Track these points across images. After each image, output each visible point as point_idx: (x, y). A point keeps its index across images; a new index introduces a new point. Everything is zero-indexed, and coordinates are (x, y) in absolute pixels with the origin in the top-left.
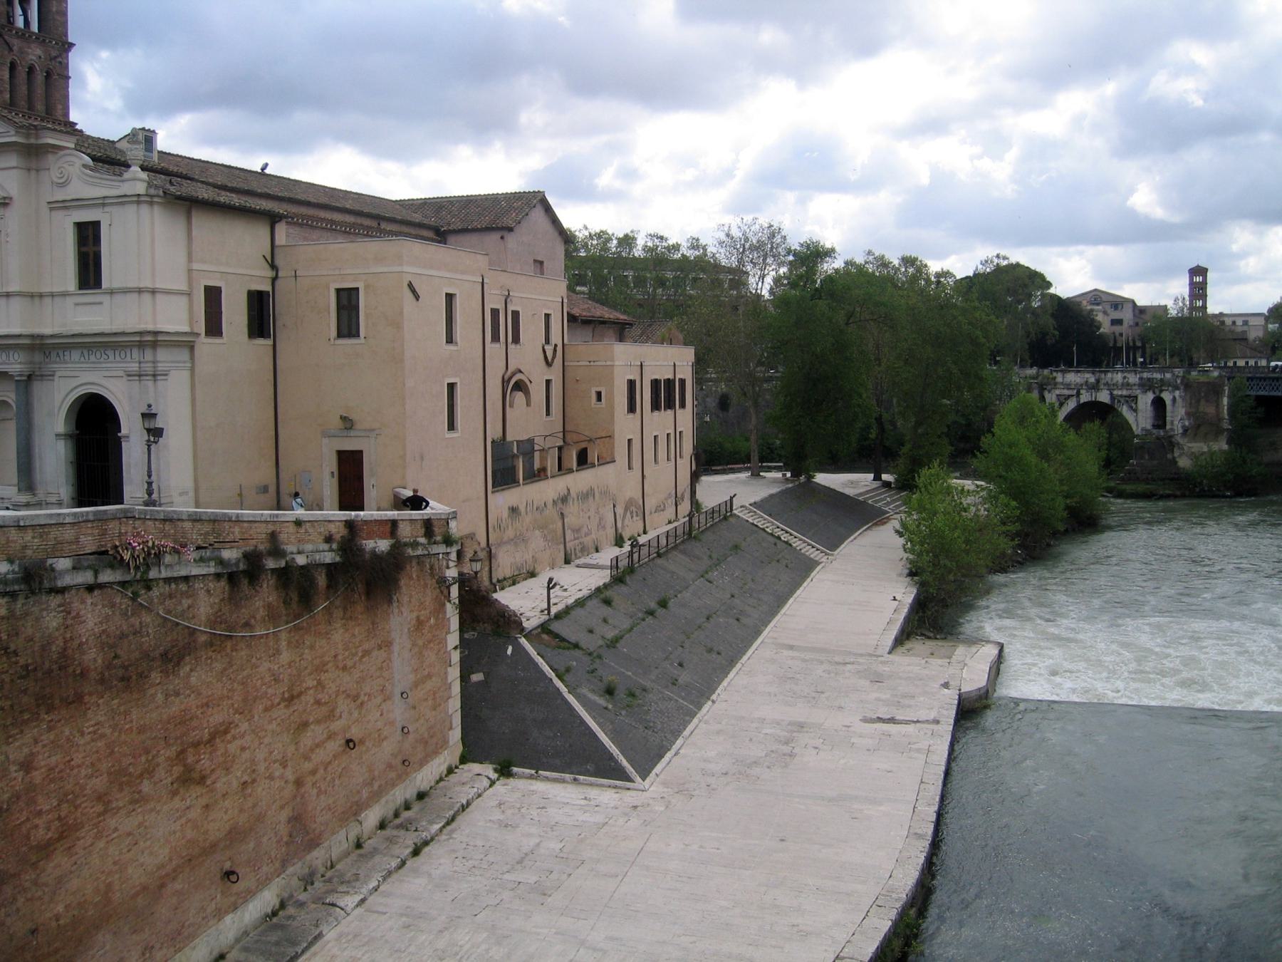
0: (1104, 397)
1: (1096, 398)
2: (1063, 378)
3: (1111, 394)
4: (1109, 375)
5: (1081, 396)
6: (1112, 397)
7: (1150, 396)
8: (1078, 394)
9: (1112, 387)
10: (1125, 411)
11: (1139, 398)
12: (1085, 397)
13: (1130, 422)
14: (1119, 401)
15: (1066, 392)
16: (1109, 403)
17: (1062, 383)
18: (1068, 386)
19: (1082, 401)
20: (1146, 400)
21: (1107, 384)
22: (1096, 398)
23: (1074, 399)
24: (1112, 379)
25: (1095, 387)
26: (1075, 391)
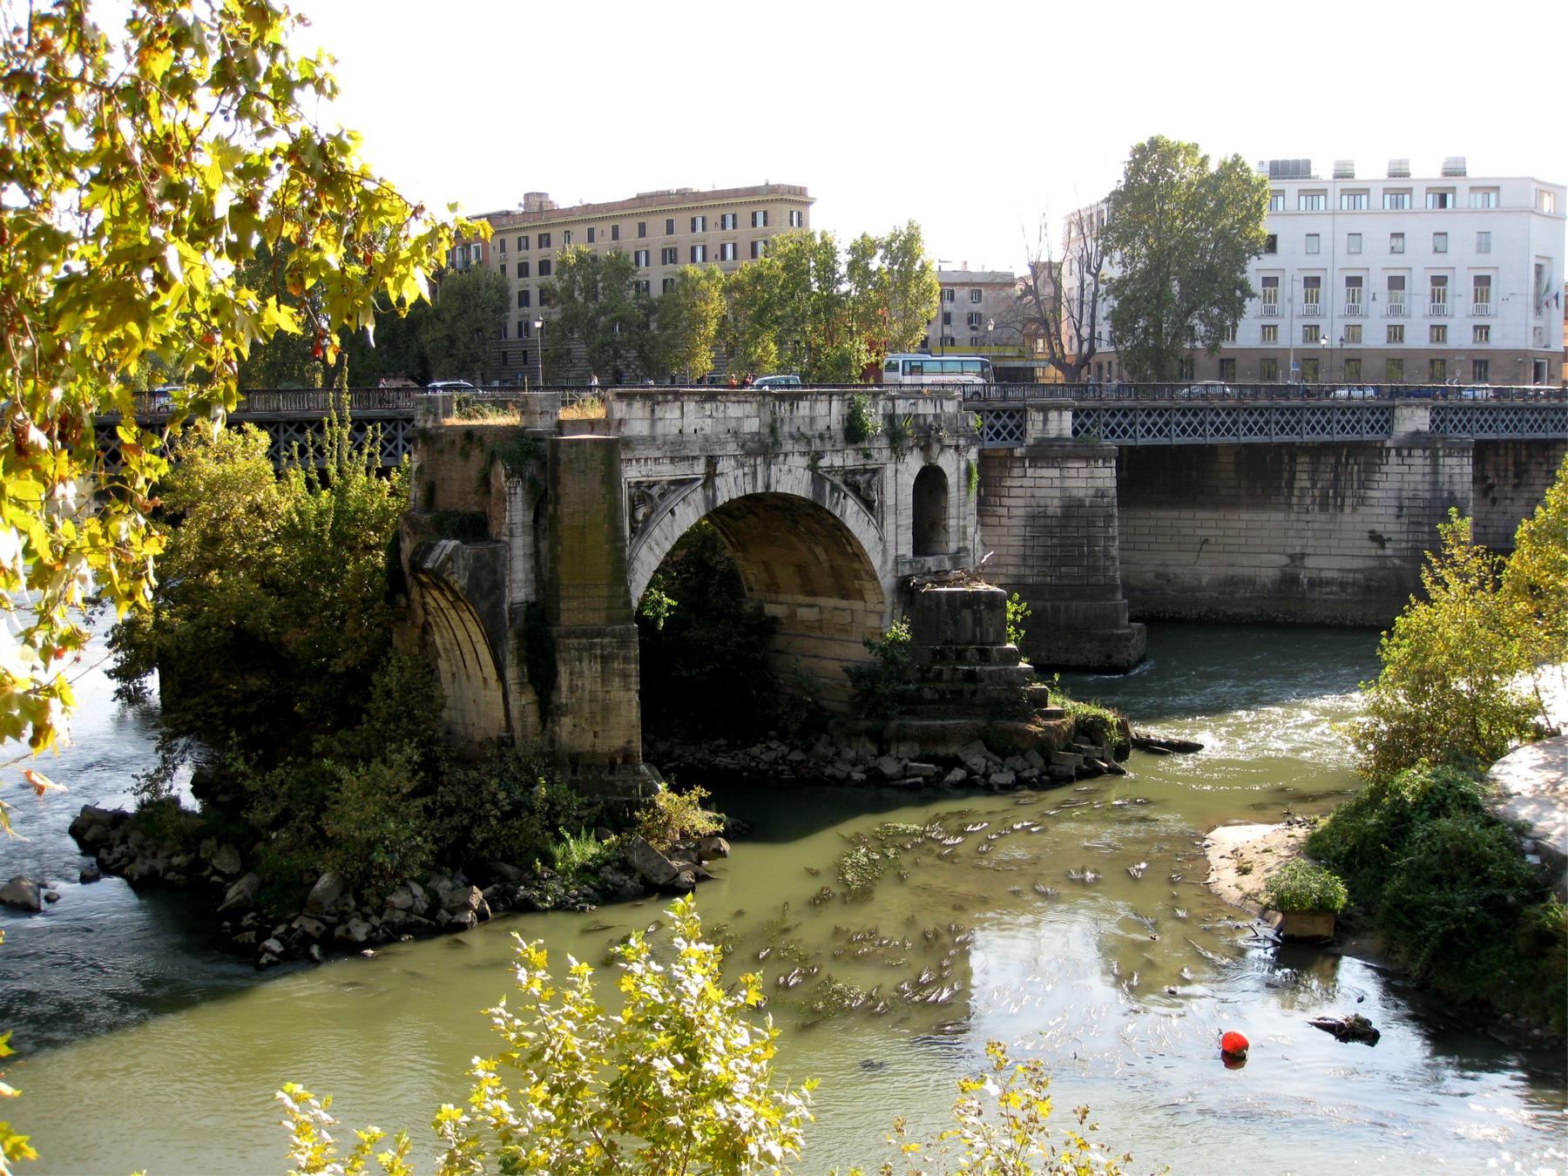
0: (792, 479)
1: (768, 486)
2: (653, 422)
3: (813, 467)
4: (804, 408)
5: (718, 481)
6: (818, 478)
7: (913, 464)
8: (711, 476)
9: (817, 445)
10: (851, 514)
11: (889, 471)
12: (731, 487)
13: (866, 547)
14: (834, 488)
15: (667, 472)
16: (810, 496)
17: (652, 439)
18: (677, 450)
19: (722, 498)
20: (901, 478)
21: (800, 437)
22: (768, 486)
23: (697, 496)
24: (812, 420)
25: (765, 448)
26: (700, 468)
